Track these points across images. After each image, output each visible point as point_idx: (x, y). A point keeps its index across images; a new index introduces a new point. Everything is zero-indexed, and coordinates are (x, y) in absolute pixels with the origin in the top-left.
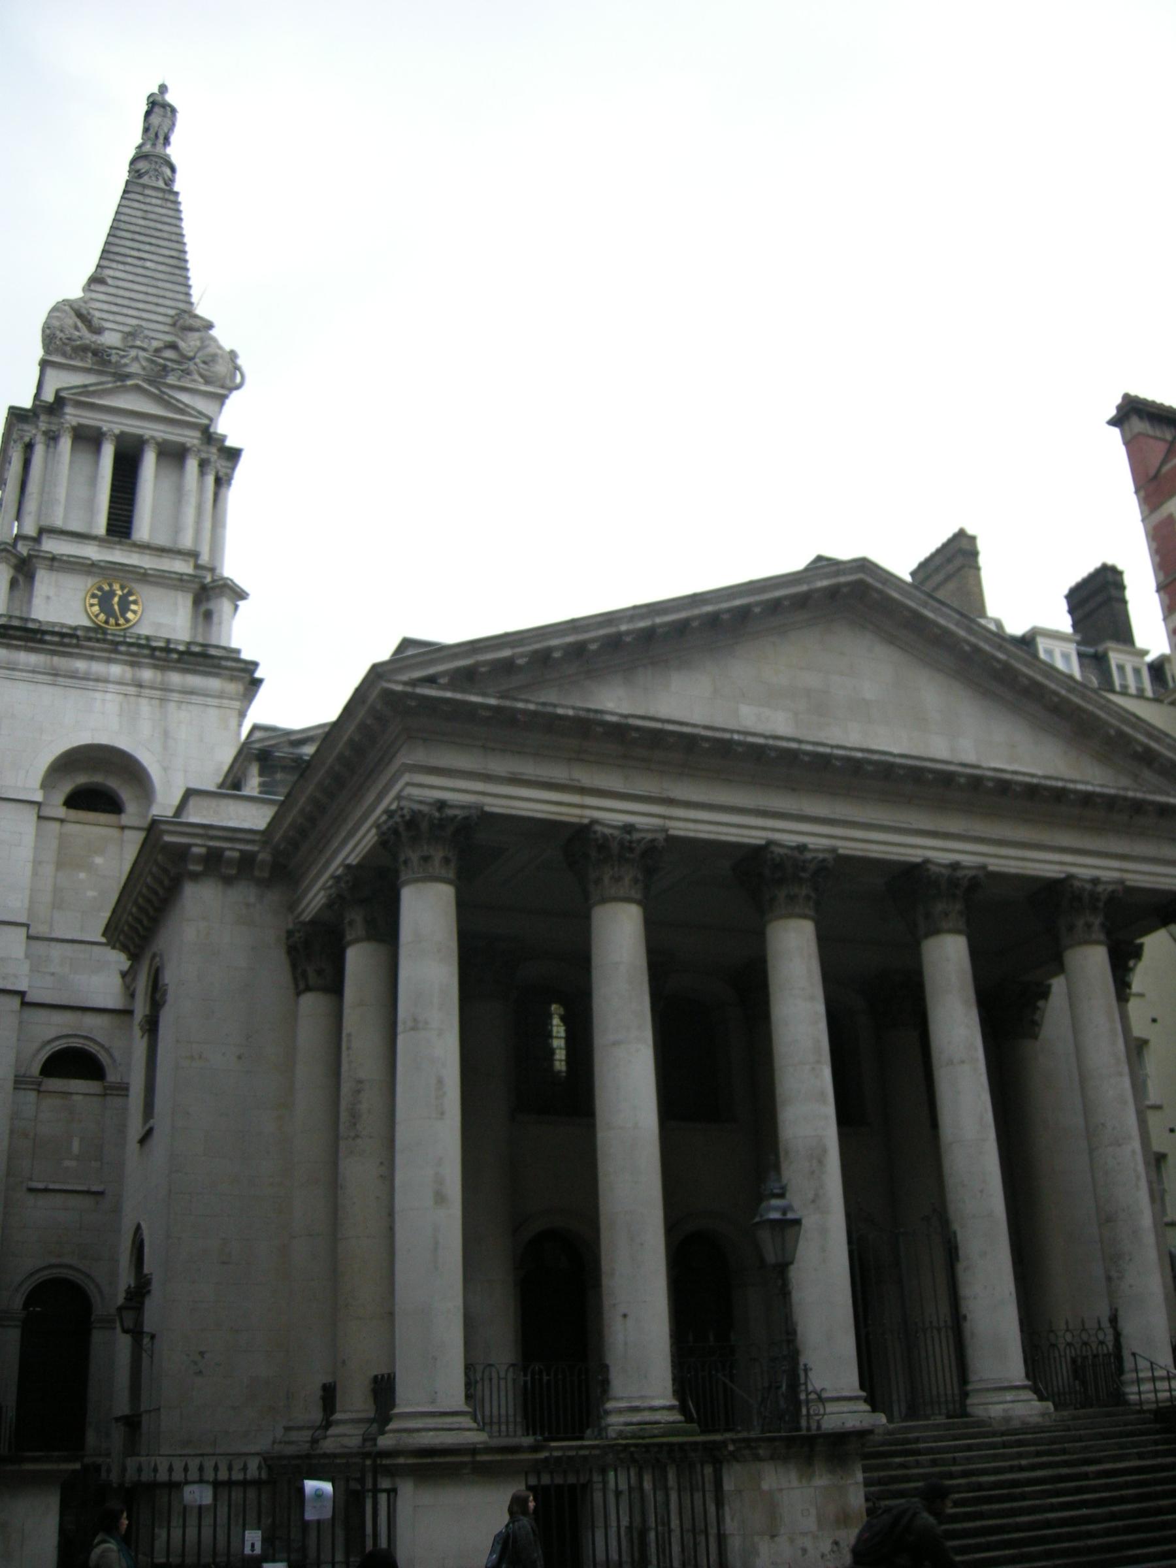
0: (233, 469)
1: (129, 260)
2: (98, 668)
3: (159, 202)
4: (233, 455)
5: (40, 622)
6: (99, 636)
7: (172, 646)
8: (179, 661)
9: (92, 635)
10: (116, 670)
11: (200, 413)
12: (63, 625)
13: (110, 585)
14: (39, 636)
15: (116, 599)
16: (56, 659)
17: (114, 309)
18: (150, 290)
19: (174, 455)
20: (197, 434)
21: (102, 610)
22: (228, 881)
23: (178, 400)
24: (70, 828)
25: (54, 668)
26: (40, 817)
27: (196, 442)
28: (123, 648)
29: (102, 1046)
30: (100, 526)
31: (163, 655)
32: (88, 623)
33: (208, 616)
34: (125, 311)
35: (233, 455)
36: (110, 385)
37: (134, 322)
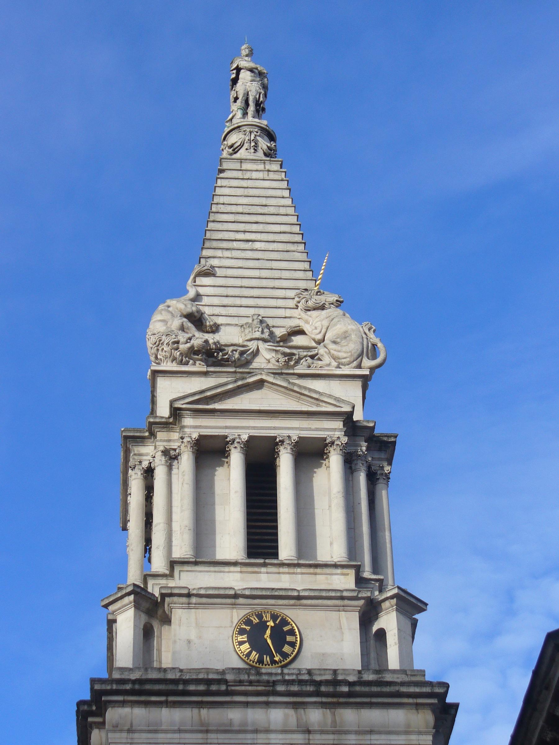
1: (235, 245)
2: (255, 716)
3: (260, 175)
5: (181, 671)
6: (252, 678)
7: (340, 677)
8: (349, 695)
9: (245, 677)
10: (277, 716)
11: (337, 399)
12: (208, 671)
13: (260, 616)
14: (181, 687)
15: (268, 632)
16: (204, 712)
17: (226, 301)
18: (264, 273)
20: (339, 424)
21: (253, 647)
23: (310, 390)
25: (202, 724)
27: (340, 434)
28: (281, 688)
31: (331, 689)
32: (241, 665)
33: (381, 634)
34: (238, 301)
36: (230, 386)
37: (251, 311)
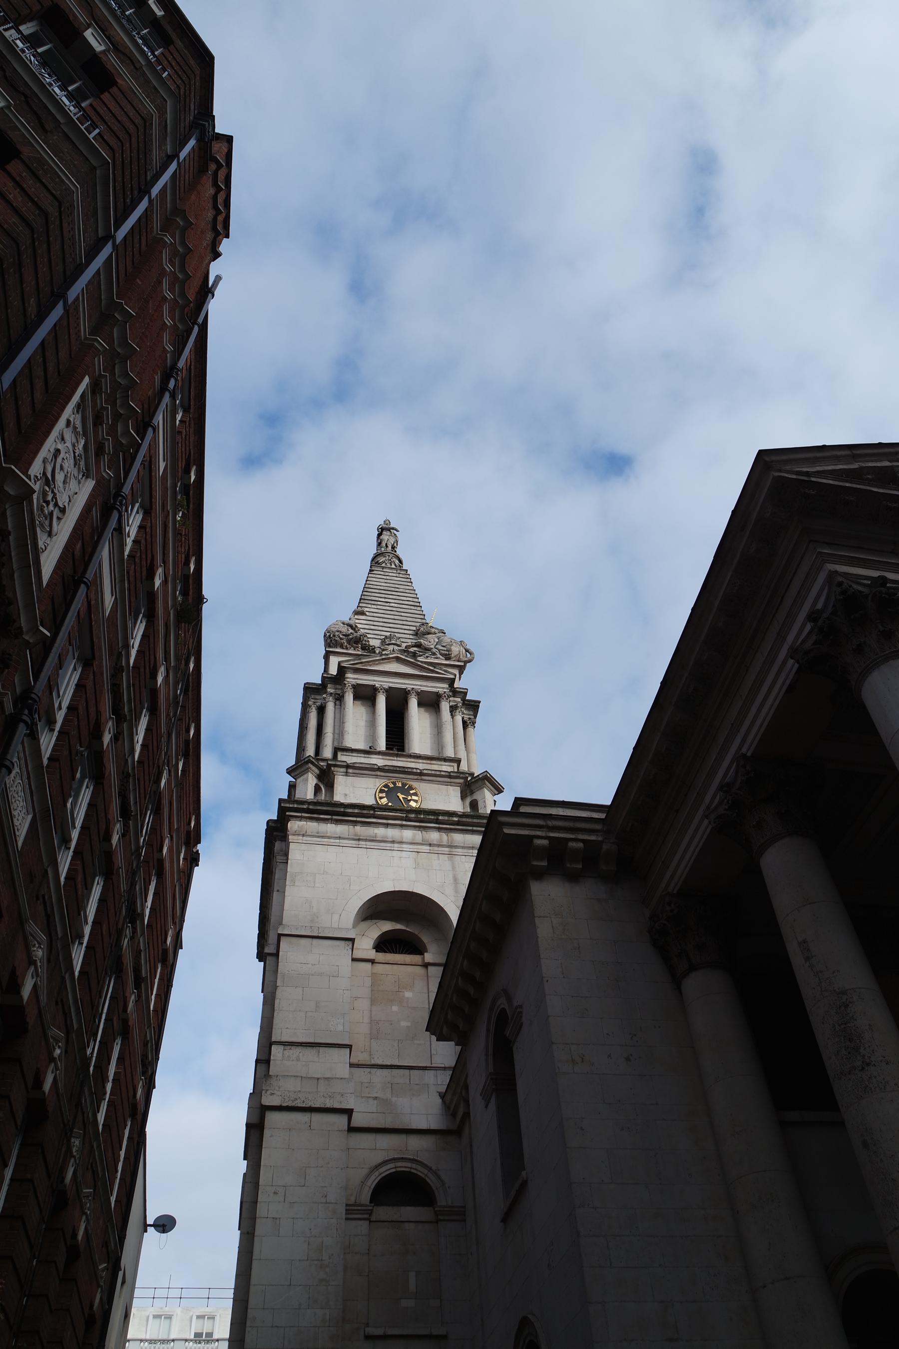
0: (475, 717)
2: (391, 833)
4: (474, 706)
19: (431, 703)
22: (573, 878)
24: (379, 968)
26: (353, 960)
29: (430, 1169)
30: (382, 745)
35: (474, 706)
